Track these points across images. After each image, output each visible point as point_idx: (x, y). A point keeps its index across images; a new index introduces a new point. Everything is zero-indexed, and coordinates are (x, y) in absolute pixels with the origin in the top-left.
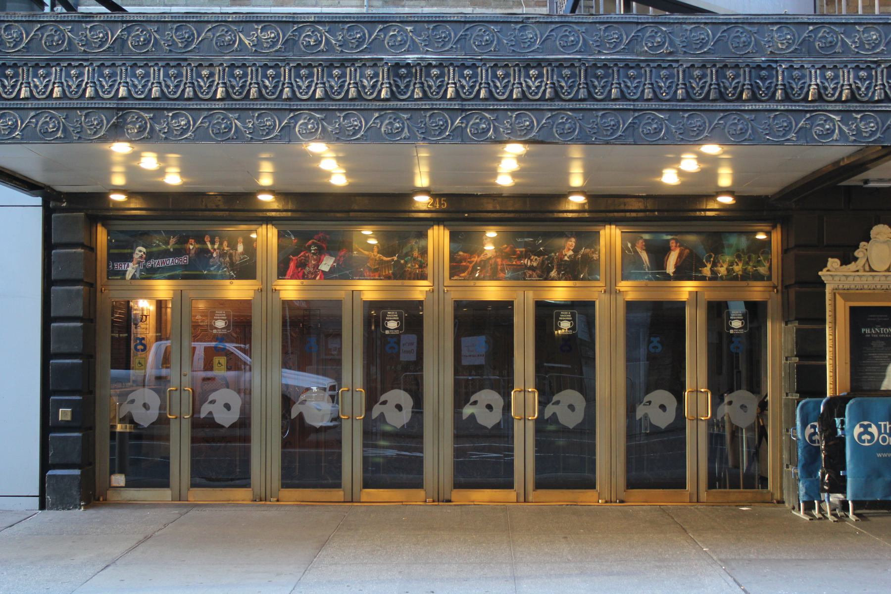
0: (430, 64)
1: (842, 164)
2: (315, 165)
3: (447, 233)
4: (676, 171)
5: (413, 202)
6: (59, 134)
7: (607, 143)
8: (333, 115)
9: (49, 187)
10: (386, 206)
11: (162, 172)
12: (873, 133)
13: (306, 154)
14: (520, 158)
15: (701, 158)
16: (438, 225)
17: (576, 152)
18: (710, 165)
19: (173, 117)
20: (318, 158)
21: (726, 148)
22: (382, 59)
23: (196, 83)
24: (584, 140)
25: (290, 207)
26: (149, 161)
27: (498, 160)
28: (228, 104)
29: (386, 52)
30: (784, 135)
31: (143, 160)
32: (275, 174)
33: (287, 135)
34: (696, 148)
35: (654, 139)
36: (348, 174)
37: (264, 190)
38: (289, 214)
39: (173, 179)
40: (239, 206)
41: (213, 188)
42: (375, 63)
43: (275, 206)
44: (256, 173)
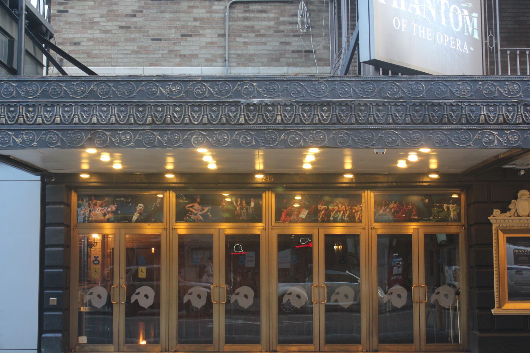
0: (267, 104)
1: (500, 157)
2: (200, 159)
3: (273, 195)
4: (405, 161)
5: (254, 178)
6: (59, 144)
7: (367, 148)
8: (210, 132)
9: (45, 170)
10: (237, 180)
11: (111, 163)
12: (516, 142)
13: (196, 153)
14: (316, 155)
15: (420, 155)
16: (269, 191)
17: (348, 152)
18: (425, 159)
19: (123, 134)
20: (202, 155)
21: (433, 150)
22: (240, 101)
23: (135, 115)
24: (354, 146)
25: (183, 181)
26: (105, 157)
27: (305, 156)
28: (153, 127)
29: (242, 97)
30: (466, 143)
31: (102, 156)
32: (175, 163)
33: (187, 144)
34: (417, 150)
35: (393, 145)
36: (217, 164)
37: (169, 172)
38: (183, 185)
39: (118, 166)
40: (154, 180)
41: (138, 171)
42: (237, 104)
43: (175, 181)
44: (164, 163)
